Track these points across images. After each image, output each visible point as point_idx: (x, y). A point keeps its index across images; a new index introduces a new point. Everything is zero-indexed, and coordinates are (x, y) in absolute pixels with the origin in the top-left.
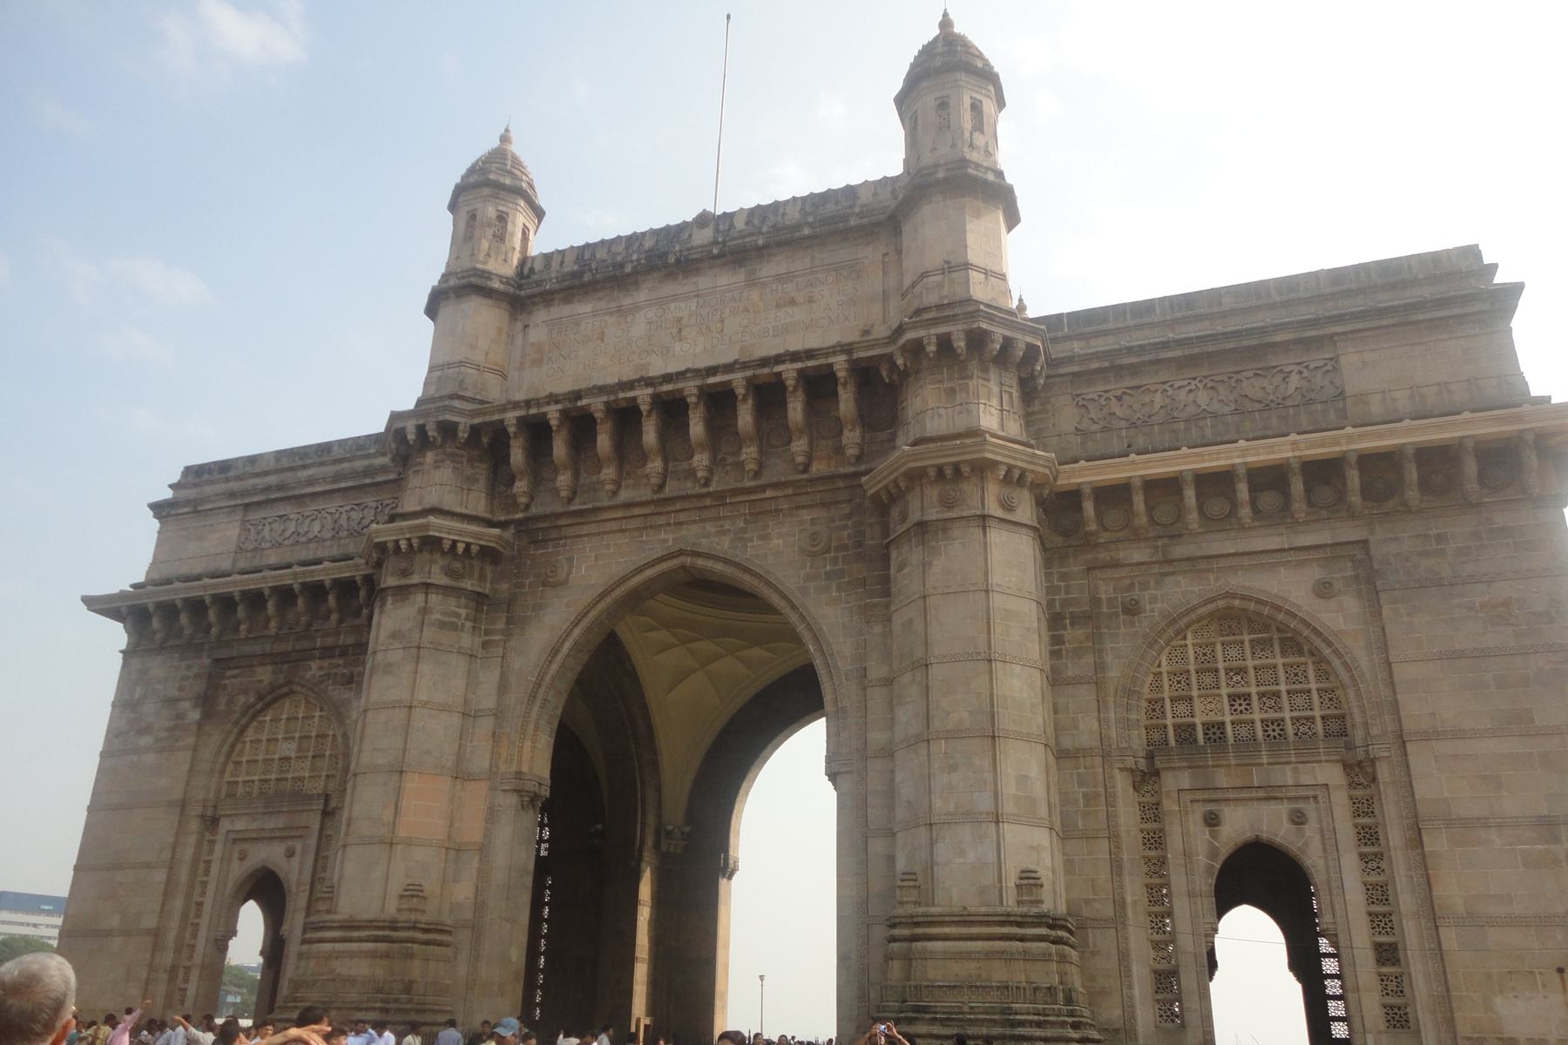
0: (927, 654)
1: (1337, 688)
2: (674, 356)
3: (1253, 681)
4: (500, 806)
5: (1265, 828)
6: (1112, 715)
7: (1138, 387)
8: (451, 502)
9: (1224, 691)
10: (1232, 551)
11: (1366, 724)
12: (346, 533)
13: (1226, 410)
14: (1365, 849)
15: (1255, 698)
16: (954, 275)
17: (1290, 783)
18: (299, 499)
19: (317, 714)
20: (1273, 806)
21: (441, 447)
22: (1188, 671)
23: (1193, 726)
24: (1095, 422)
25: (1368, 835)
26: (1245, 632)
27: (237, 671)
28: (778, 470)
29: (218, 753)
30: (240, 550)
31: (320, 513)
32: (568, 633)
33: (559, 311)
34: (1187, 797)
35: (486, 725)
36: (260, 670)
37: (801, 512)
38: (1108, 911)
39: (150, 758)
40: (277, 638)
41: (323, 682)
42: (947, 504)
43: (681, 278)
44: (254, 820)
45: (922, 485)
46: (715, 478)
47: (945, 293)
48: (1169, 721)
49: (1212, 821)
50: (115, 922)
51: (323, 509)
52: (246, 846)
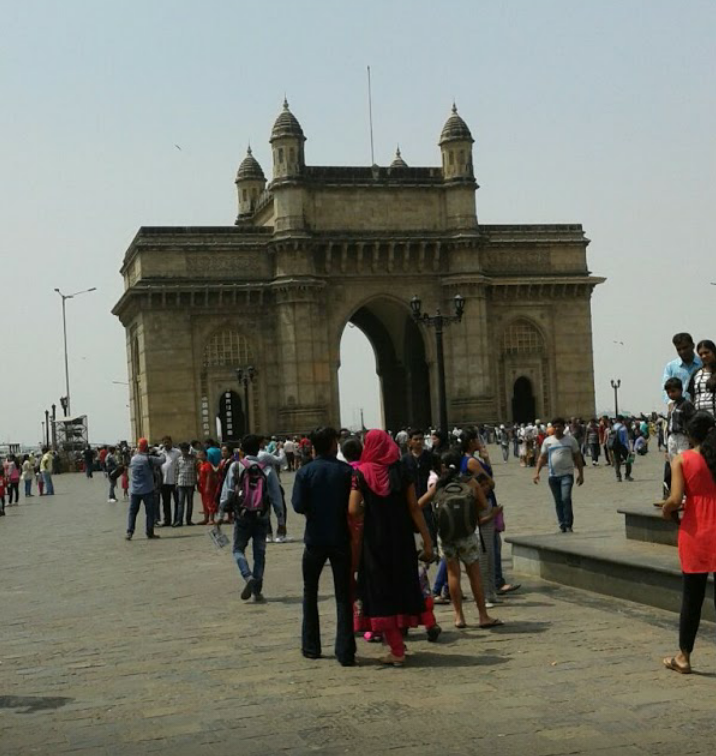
9: (518, 340)
18: (213, 252)
25: (544, 375)
30: (187, 270)
33: (326, 196)
39: (171, 352)
42: (472, 293)
48: (505, 347)
49: (514, 372)
50: (175, 410)
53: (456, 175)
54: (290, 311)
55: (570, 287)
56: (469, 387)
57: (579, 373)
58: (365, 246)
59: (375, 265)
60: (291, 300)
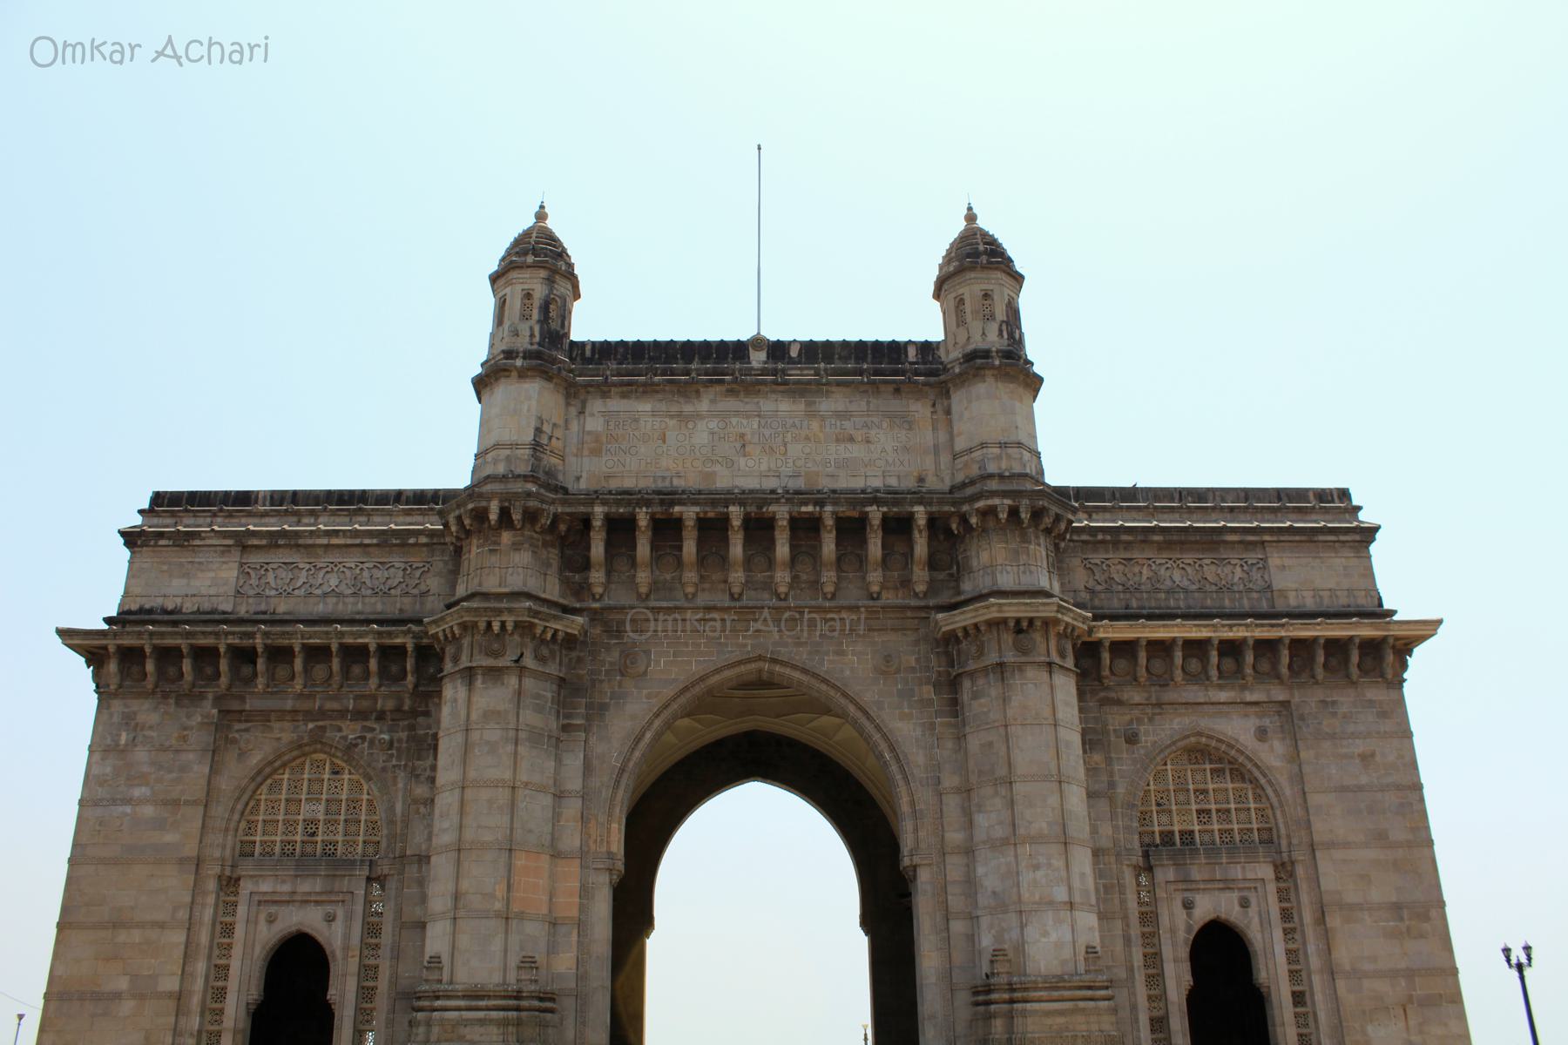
0: (1011, 774)
1: (1267, 808)
2: (739, 470)
3: (1213, 801)
4: (593, 884)
5: (1223, 910)
6: (1121, 823)
7: (1131, 559)
8: (533, 585)
9: (1194, 807)
10: (1202, 700)
11: (1288, 836)
12: (369, 592)
13: (1194, 587)
14: (1287, 925)
15: (1214, 813)
16: (1010, 451)
17: (1240, 877)
19: (346, 776)
20: (1228, 894)
21: (519, 529)
22: (1168, 790)
23: (1172, 833)
24: (1099, 584)
25: (1286, 915)
26: (1207, 762)
27: (249, 724)
28: (852, 594)
29: (233, 810)
31: (336, 566)
32: (650, 723)
33: (616, 404)
34: (1172, 887)
35: (572, 807)
36: (276, 725)
37: (871, 633)
38: (1122, 974)
39: (148, 811)
40: (300, 696)
41: (356, 745)
42: (1024, 652)
43: (742, 396)
44: (283, 882)
45: (999, 629)
46: (792, 593)
47: (1004, 465)
48: (1157, 829)
49: (1188, 906)
51: (340, 563)
52: (273, 909)
53: (971, 347)
54: (462, 693)
55: (1337, 648)
56: (1020, 947)
57: (1397, 908)
58: (697, 513)
59: (737, 576)
60: (465, 662)
